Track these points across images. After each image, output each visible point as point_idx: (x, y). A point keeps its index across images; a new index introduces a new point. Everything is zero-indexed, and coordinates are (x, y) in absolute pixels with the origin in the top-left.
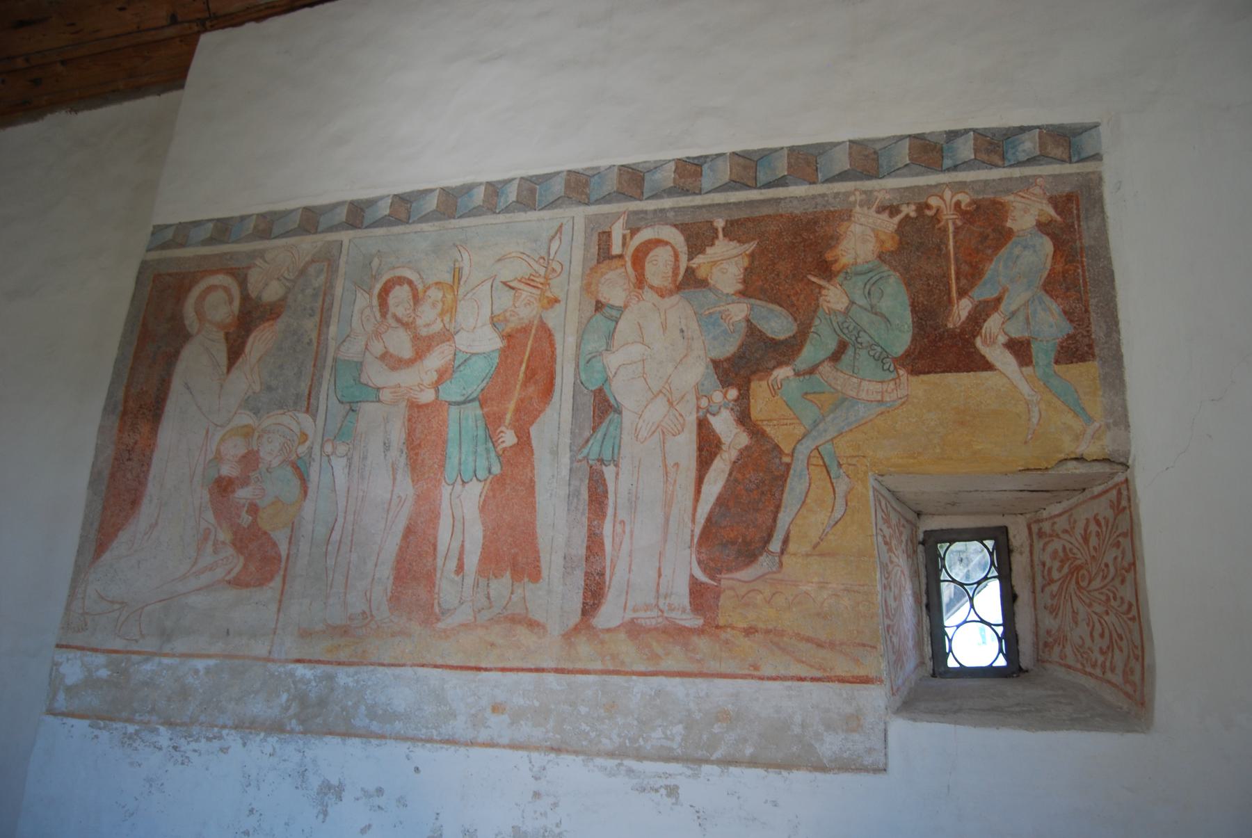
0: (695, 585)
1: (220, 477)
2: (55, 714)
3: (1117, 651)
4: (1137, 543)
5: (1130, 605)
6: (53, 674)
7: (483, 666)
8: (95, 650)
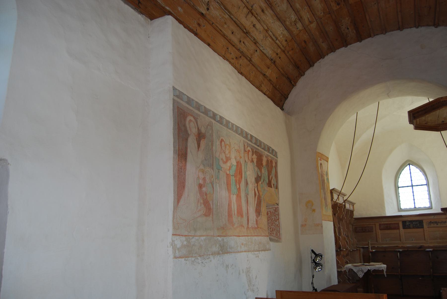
0: (256, 219)
1: (200, 183)
2: (176, 258)
3: (274, 231)
4: (279, 216)
5: (277, 225)
6: (173, 244)
7: (240, 235)
8: (182, 236)
